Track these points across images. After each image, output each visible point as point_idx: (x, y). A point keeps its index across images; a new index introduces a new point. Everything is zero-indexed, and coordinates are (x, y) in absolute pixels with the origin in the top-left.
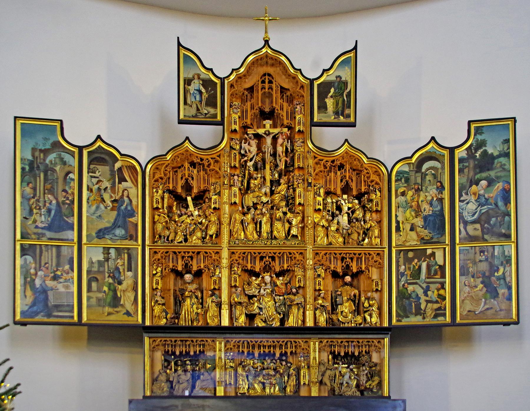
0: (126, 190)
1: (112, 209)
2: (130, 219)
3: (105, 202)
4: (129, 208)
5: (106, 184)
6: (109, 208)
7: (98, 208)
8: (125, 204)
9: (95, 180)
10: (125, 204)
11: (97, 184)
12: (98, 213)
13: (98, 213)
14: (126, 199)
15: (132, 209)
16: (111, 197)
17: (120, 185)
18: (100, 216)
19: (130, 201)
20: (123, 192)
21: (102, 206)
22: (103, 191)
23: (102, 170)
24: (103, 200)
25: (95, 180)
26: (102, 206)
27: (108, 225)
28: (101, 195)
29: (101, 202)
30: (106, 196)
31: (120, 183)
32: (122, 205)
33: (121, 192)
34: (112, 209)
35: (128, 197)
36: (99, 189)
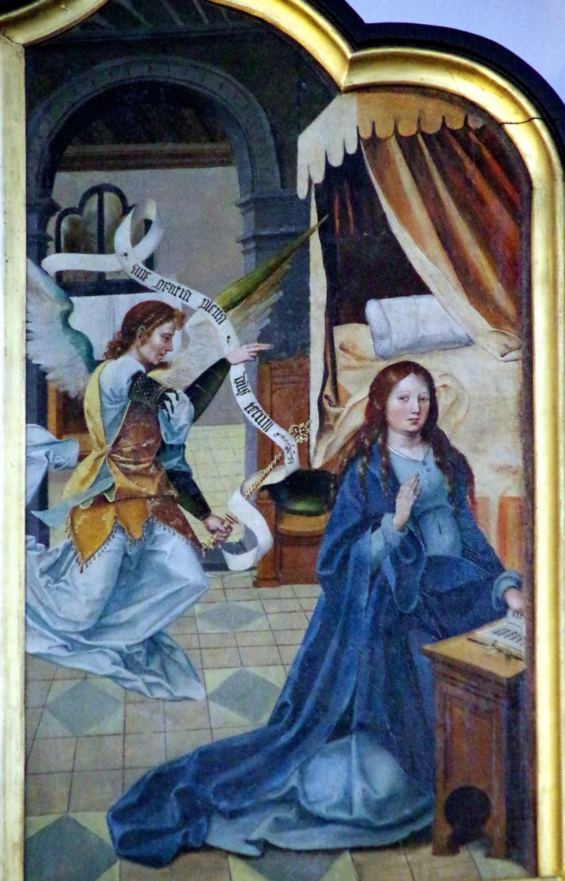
0: (405, 368)
1: (275, 570)
2: (456, 648)
3: (202, 510)
4: (441, 540)
5: (214, 336)
6: (240, 563)
7: (132, 570)
8: (404, 503)
9: (100, 317)
10: (404, 503)
11: (118, 349)
12: (140, 620)
13: (140, 620)
14: (408, 458)
15: (474, 548)
16: (264, 452)
17: (344, 333)
18: (154, 644)
19: (456, 469)
20: (380, 389)
21: (174, 552)
22: (181, 409)
23: (179, 218)
24: (185, 496)
25: (100, 317)
26: (174, 552)
27: (233, 723)
28: (163, 450)
29: (166, 514)
30: (218, 456)
31: (346, 308)
32: (372, 521)
33: (356, 391)
34: (275, 570)
35: (429, 432)
36: (145, 393)
